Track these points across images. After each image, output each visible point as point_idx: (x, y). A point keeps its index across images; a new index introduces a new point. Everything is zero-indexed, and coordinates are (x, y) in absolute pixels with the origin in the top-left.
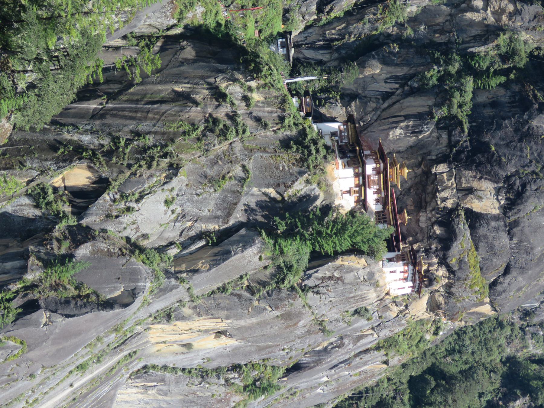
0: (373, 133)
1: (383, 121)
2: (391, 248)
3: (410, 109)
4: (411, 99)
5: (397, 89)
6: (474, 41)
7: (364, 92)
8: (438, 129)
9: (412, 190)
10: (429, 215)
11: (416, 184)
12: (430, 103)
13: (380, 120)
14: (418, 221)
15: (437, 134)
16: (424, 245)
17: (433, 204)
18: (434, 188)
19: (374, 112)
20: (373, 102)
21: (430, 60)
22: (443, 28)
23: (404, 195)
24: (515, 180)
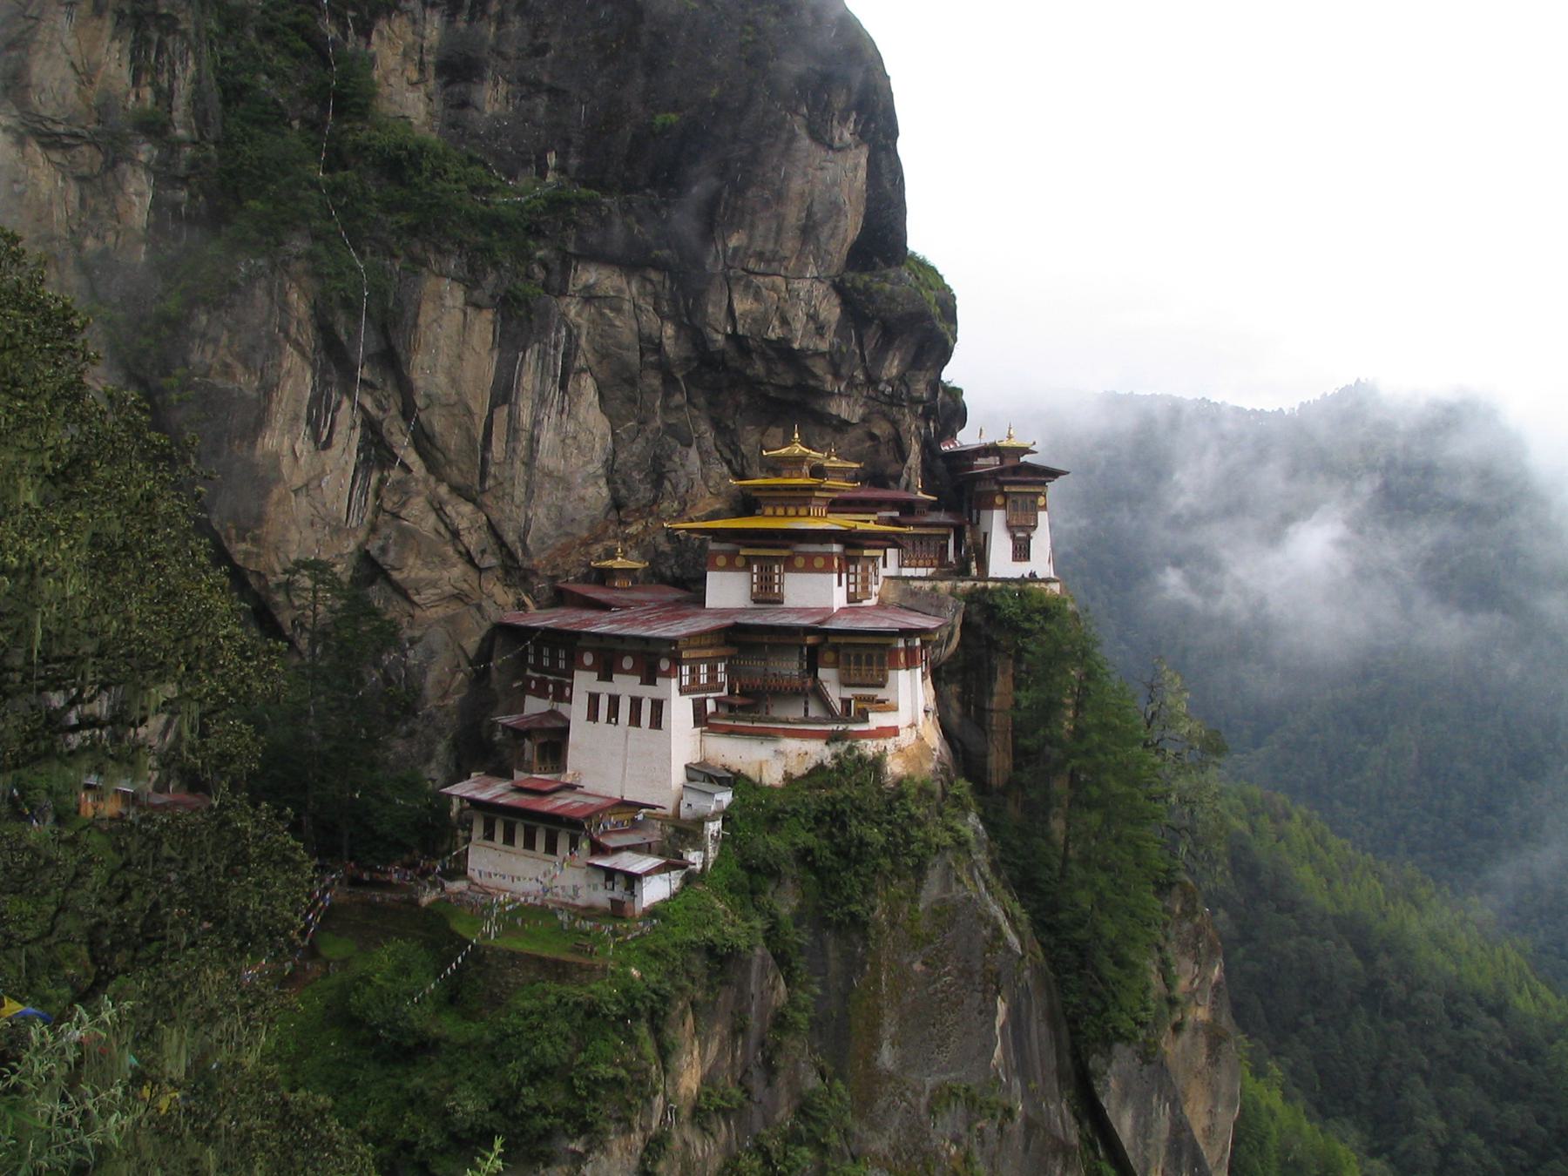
1: (490, 483)
2: (943, 531)
3: (469, 374)
6: (164, 80)
8: (565, 295)
9: (730, 423)
11: (710, 403)
12: (454, 296)
13: (483, 491)
14: (843, 426)
16: (908, 418)
17: (819, 367)
18: (763, 356)
19: (448, 509)
20: (404, 504)
22: (81, 179)
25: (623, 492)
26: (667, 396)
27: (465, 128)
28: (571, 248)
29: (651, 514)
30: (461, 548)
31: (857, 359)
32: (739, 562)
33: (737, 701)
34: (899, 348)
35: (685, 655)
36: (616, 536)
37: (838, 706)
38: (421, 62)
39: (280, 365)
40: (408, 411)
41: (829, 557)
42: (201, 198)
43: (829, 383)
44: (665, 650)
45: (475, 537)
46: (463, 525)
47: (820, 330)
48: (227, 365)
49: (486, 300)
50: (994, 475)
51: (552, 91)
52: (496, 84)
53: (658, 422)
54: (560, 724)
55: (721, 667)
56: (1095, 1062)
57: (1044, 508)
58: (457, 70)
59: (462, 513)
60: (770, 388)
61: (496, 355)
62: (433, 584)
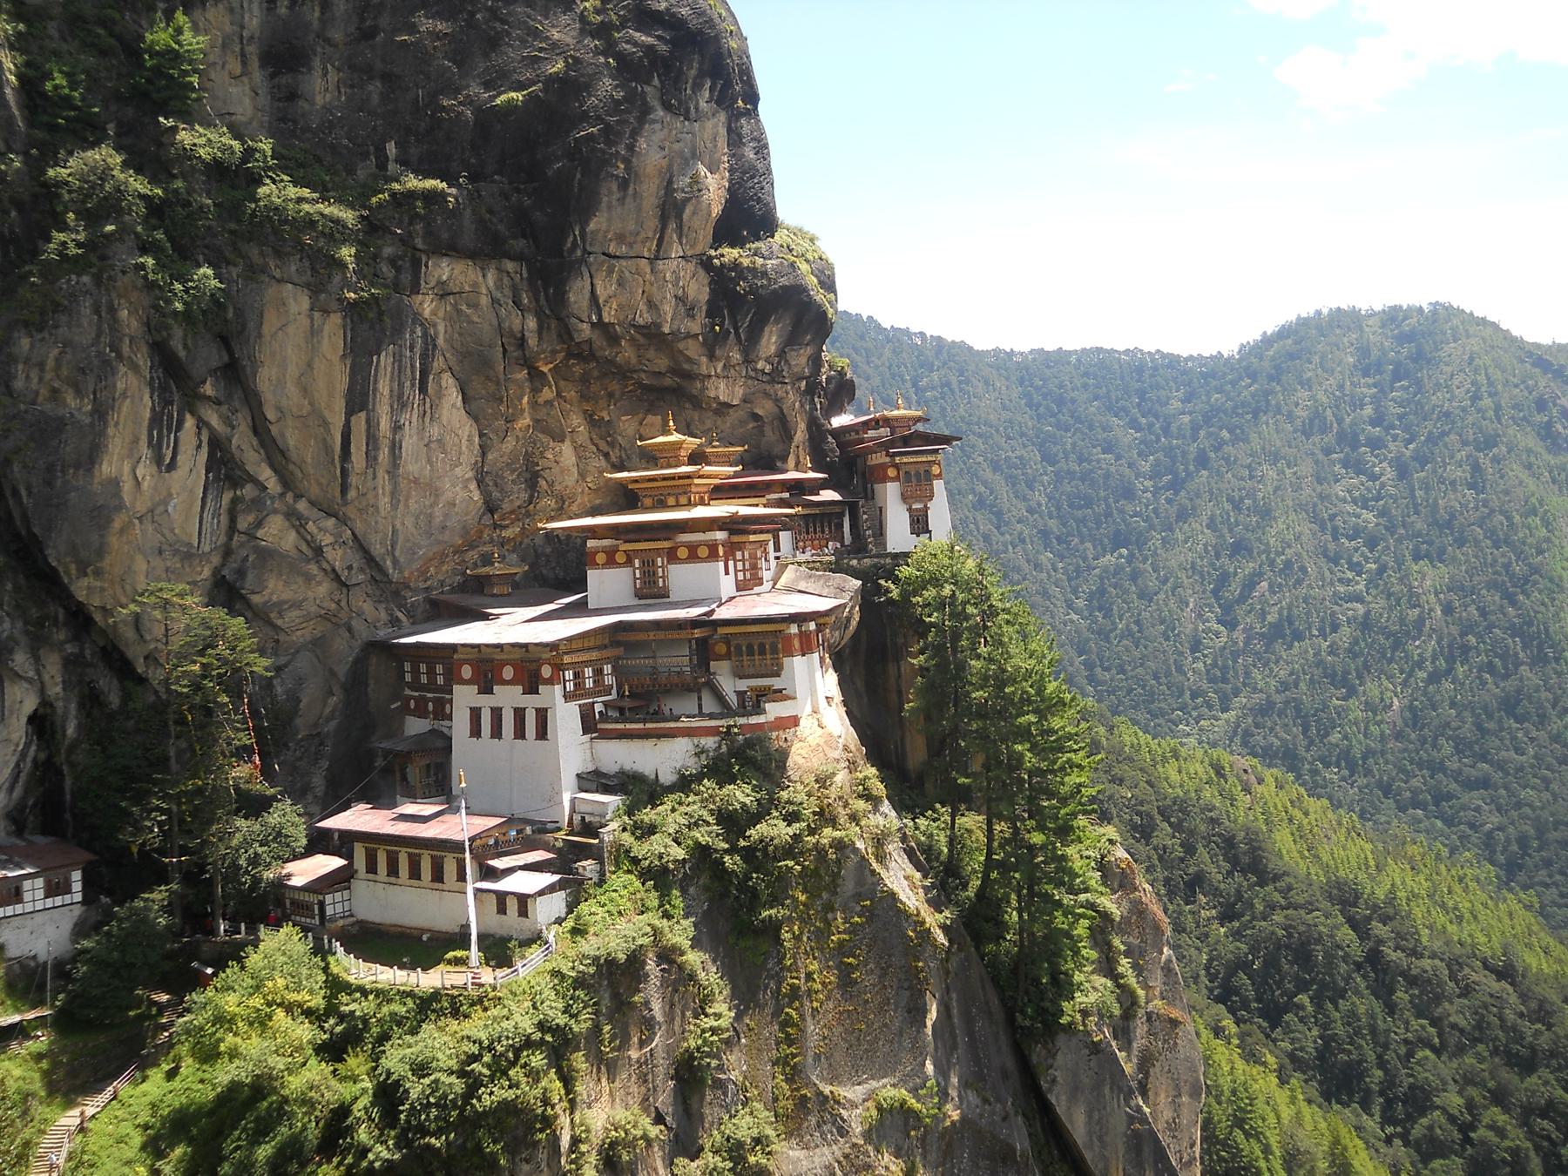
0: (401, 538)
1: (352, 494)
4: (265, 380)
5: (201, 424)
7: (204, 557)
10: (720, 366)
11: (584, 397)
12: (299, 303)
13: (346, 503)
15: (428, 298)
16: (791, 395)
17: (692, 349)
18: (633, 339)
19: (311, 526)
20: (259, 524)
21: (85, 279)
23: (611, 445)
24: (630, 41)
25: (496, 494)
26: (536, 391)
27: (295, 122)
28: (419, 243)
29: (528, 514)
30: (325, 565)
31: (732, 336)
32: (620, 558)
33: (627, 703)
34: (777, 322)
35: (567, 659)
36: (492, 541)
37: (733, 700)
38: (243, 54)
39: (115, 386)
40: (260, 428)
41: (713, 547)
42: (13, 214)
43: (704, 365)
44: (545, 656)
45: (340, 552)
46: (327, 540)
47: (690, 312)
48: (55, 391)
49: (334, 305)
50: (885, 446)
51: (387, 77)
52: (325, 74)
53: (526, 420)
54: (440, 743)
55: (607, 669)
56: (1037, 1054)
57: (939, 476)
58: (283, 58)
59: (324, 531)
60: (643, 376)
61: (348, 362)
62: (296, 605)
